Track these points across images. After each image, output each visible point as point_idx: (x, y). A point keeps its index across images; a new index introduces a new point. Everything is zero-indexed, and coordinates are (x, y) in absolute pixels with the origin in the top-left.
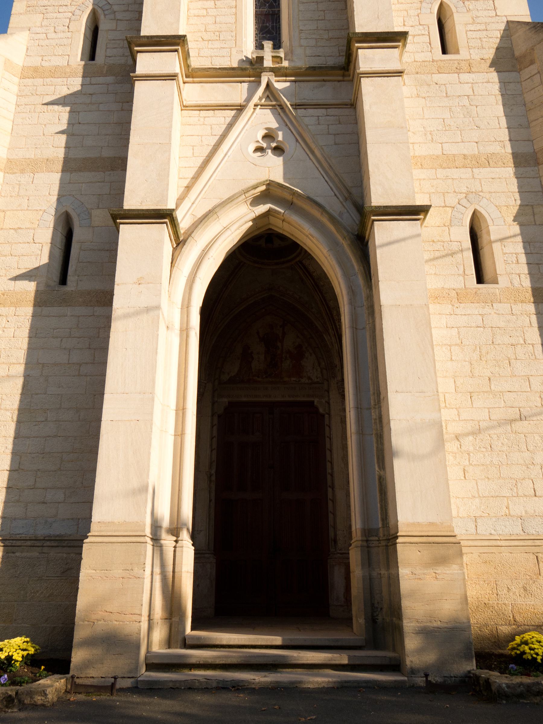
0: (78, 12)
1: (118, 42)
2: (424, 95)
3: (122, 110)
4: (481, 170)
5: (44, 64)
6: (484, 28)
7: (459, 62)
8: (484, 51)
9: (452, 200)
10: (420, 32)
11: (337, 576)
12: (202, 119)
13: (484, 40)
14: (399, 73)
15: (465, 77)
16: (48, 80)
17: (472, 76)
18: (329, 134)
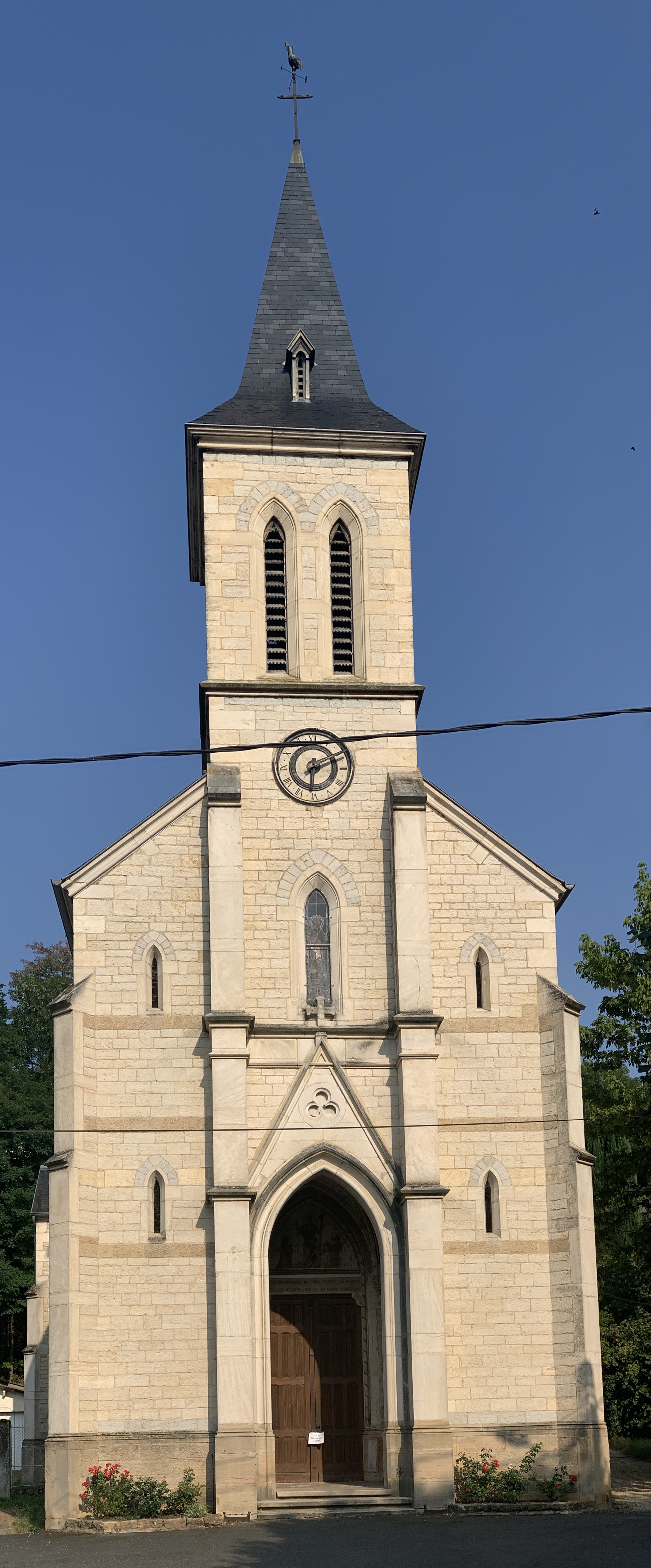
0: (138, 950)
1: (181, 988)
2: (457, 1056)
3: (193, 1067)
4: (498, 1133)
5: (116, 1013)
6: (513, 981)
7: (489, 1020)
8: (512, 1009)
9: (471, 1163)
10: (458, 985)
11: (370, 1450)
12: (264, 1078)
13: (513, 995)
14: (435, 1057)
15: (493, 1036)
16: (122, 1032)
17: (499, 1035)
18: (374, 1095)
